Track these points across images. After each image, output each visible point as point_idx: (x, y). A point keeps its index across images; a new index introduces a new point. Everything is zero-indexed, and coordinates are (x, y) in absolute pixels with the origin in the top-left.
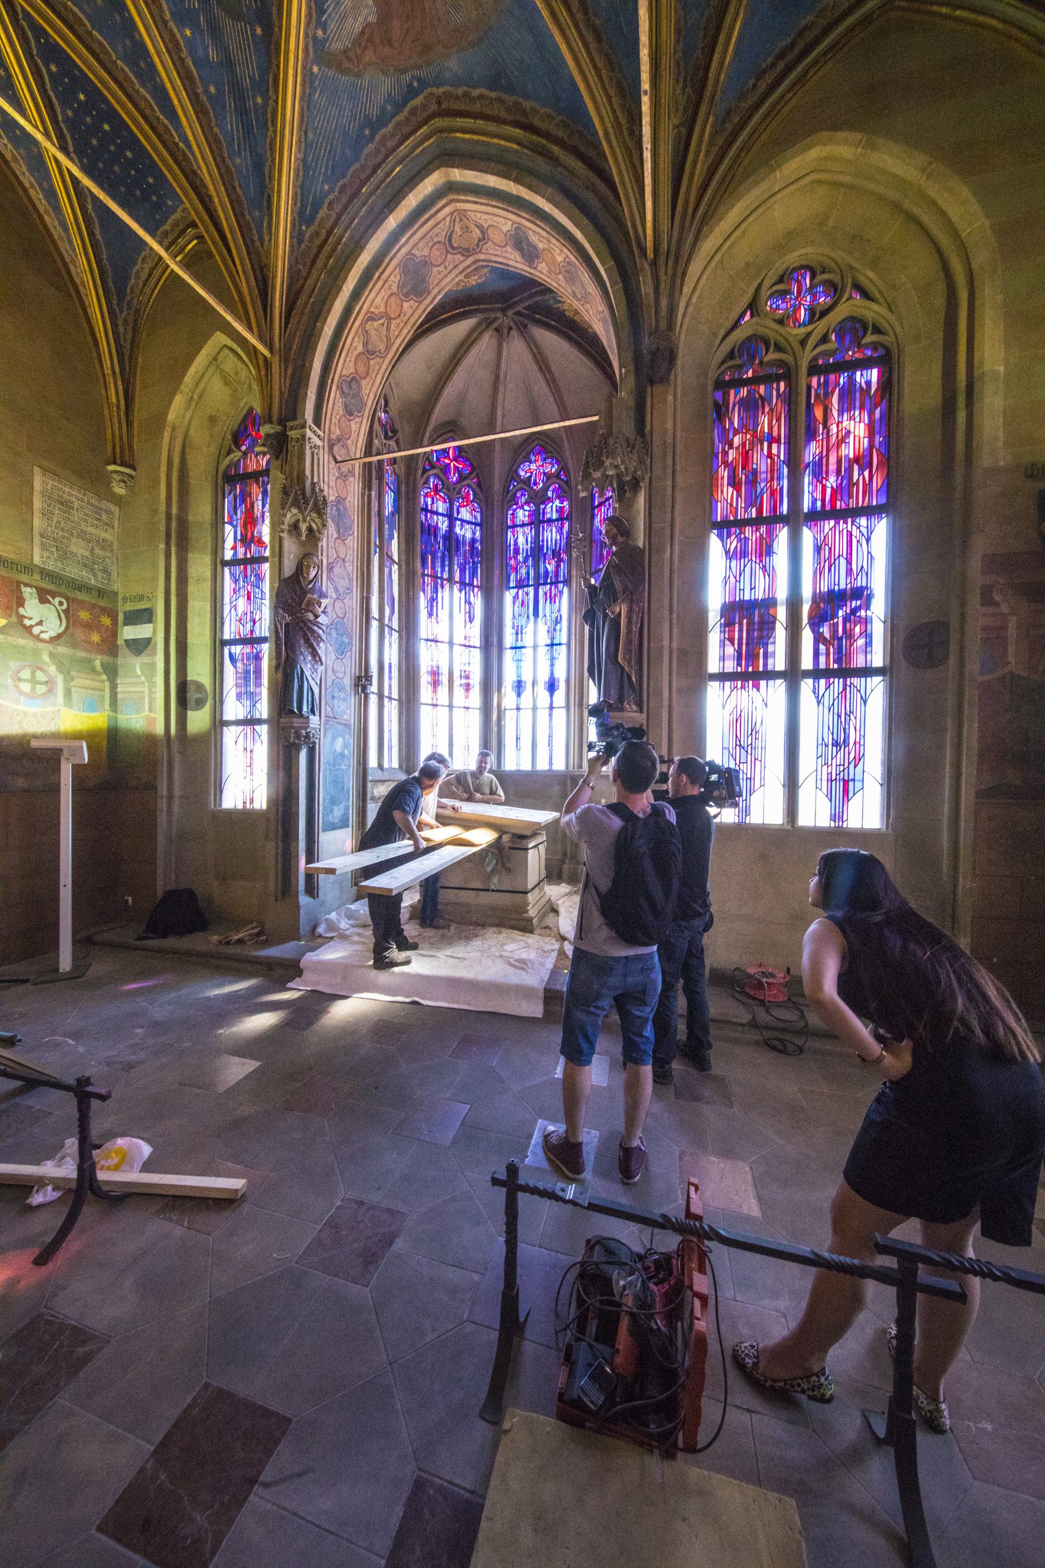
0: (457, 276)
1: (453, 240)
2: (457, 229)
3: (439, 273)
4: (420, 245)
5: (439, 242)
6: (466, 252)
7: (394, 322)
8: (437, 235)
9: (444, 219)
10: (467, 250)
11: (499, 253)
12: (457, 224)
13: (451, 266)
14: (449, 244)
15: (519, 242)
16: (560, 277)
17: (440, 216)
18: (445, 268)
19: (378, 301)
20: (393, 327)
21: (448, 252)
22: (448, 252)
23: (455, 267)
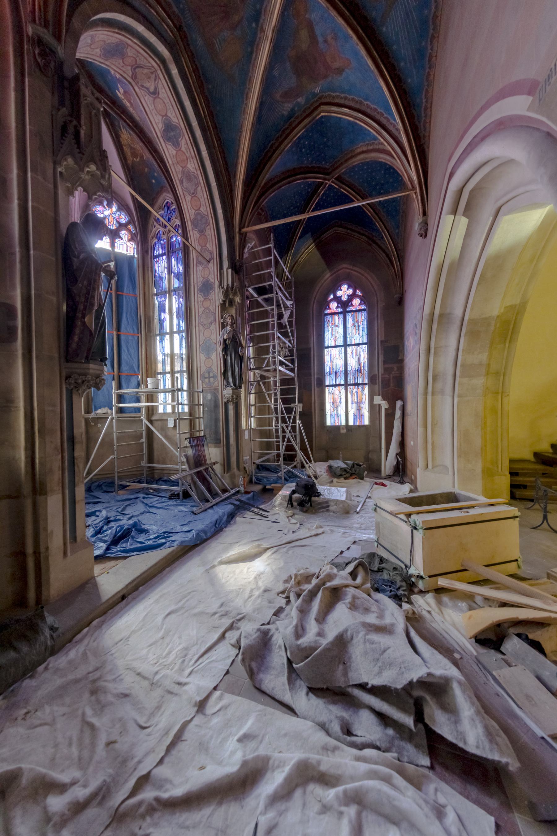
0: (119, 73)
1: (139, 69)
2: (145, 71)
3: (119, 64)
4: (133, 50)
5: (136, 61)
6: (134, 77)
7: (89, 48)
8: (140, 59)
9: (149, 62)
10: (136, 78)
11: (151, 108)
12: (148, 70)
13: (123, 69)
14: (136, 67)
15: (169, 128)
16: (181, 169)
17: (150, 60)
18: (123, 66)
19: (103, 36)
20: (85, 49)
21: (132, 66)
22: (132, 66)
23: (124, 72)
